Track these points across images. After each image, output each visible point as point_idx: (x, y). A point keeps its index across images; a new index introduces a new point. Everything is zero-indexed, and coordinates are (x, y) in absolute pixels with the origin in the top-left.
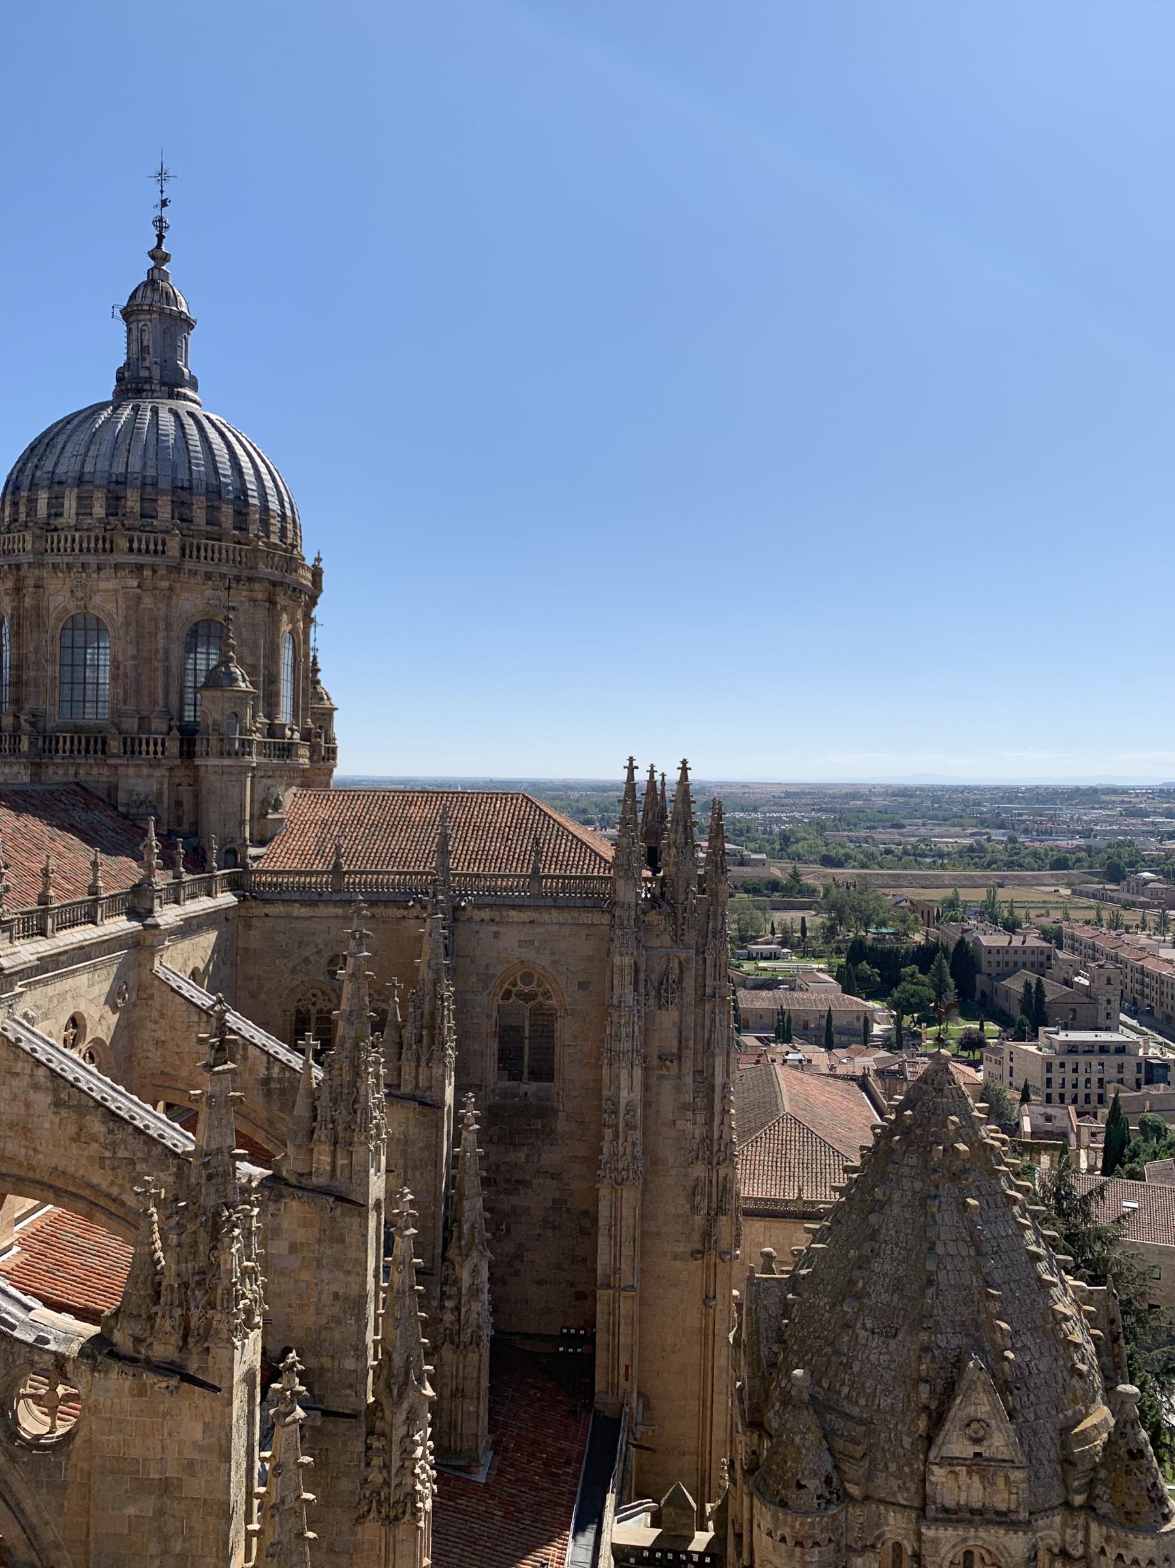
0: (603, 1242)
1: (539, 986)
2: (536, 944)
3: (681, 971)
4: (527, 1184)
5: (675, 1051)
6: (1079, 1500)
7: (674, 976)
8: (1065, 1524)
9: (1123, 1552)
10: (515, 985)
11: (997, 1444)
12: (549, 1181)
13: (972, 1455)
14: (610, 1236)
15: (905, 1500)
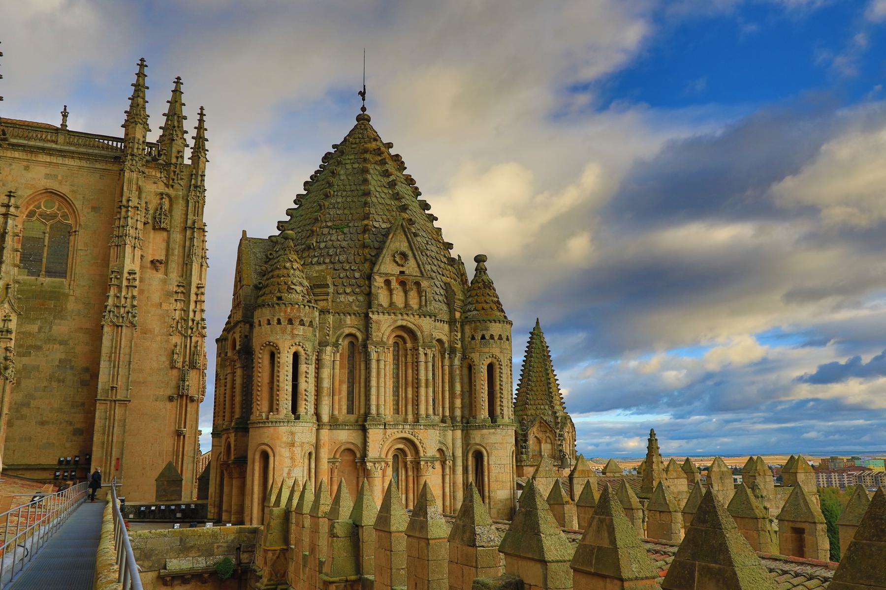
0: (104, 365)
1: (58, 209)
2: (60, 178)
3: (171, 205)
4: (38, 348)
5: (163, 258)
6: (458, 315)
7: (166, 206)
8: (451, 332)
9: (485, 332)
10: (39, 207)
11: (413, 266)
12: (57, 346)
13: (398, 273)
14: (110, 361)
15: (357, 307)
